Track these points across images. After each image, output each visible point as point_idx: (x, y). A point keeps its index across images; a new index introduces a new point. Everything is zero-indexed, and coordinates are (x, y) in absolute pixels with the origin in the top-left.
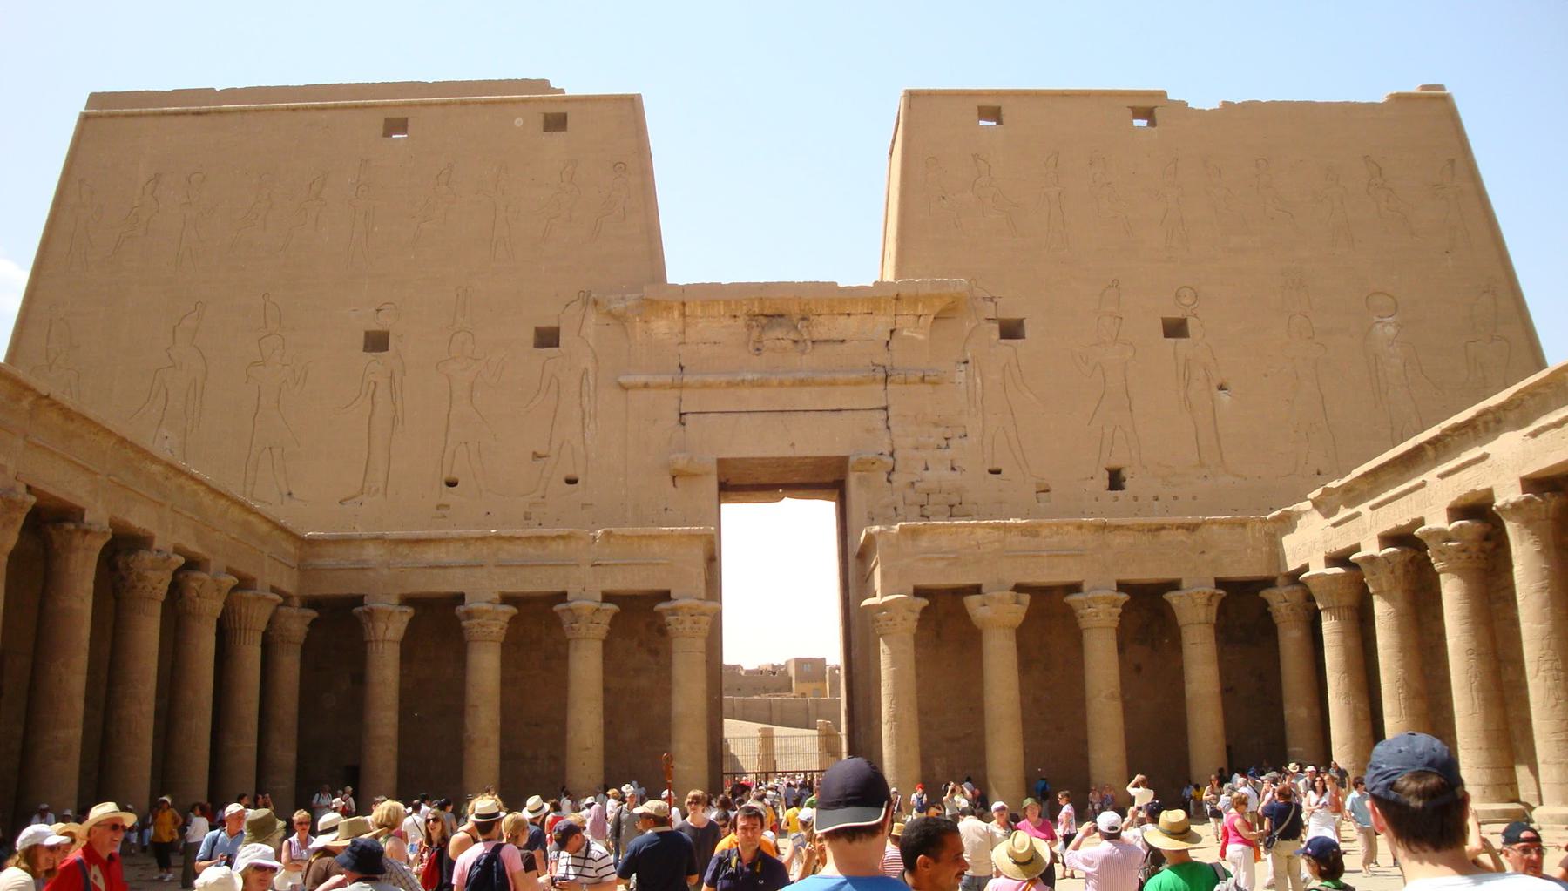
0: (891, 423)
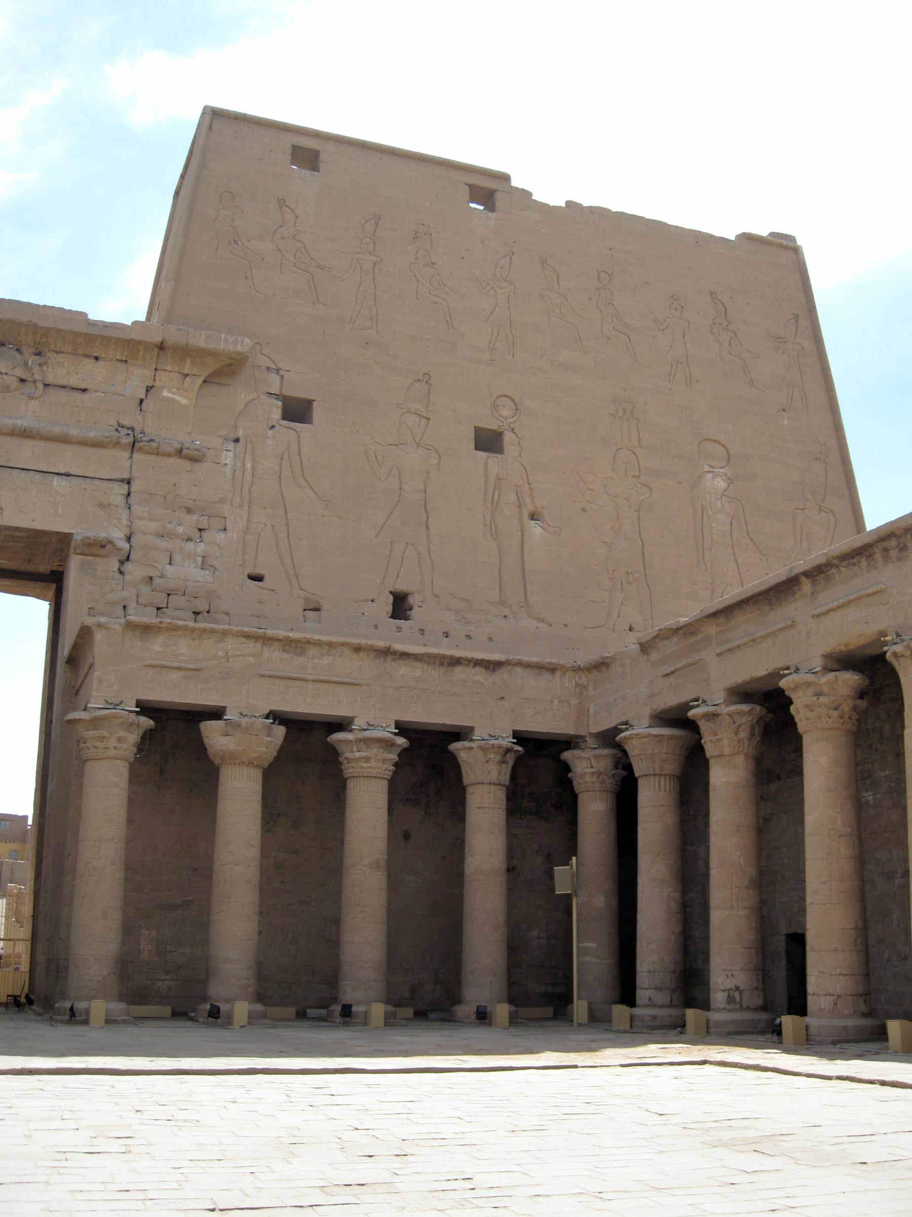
0: (133, 500)
